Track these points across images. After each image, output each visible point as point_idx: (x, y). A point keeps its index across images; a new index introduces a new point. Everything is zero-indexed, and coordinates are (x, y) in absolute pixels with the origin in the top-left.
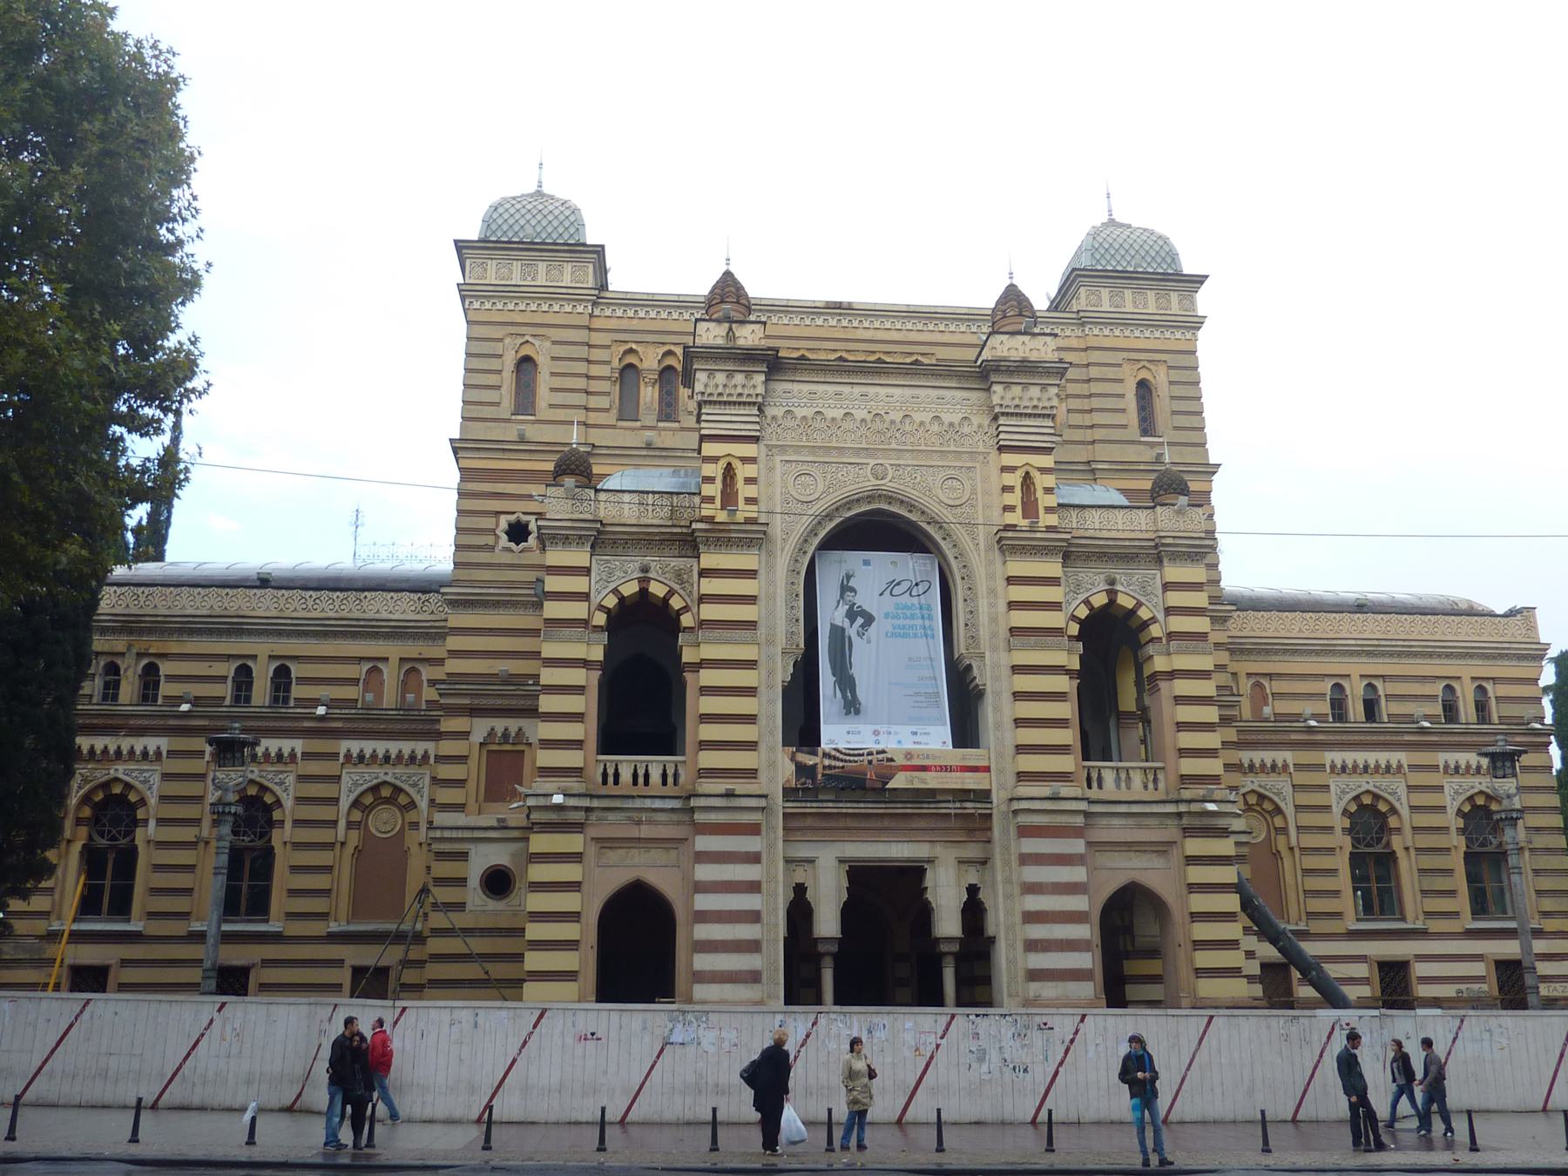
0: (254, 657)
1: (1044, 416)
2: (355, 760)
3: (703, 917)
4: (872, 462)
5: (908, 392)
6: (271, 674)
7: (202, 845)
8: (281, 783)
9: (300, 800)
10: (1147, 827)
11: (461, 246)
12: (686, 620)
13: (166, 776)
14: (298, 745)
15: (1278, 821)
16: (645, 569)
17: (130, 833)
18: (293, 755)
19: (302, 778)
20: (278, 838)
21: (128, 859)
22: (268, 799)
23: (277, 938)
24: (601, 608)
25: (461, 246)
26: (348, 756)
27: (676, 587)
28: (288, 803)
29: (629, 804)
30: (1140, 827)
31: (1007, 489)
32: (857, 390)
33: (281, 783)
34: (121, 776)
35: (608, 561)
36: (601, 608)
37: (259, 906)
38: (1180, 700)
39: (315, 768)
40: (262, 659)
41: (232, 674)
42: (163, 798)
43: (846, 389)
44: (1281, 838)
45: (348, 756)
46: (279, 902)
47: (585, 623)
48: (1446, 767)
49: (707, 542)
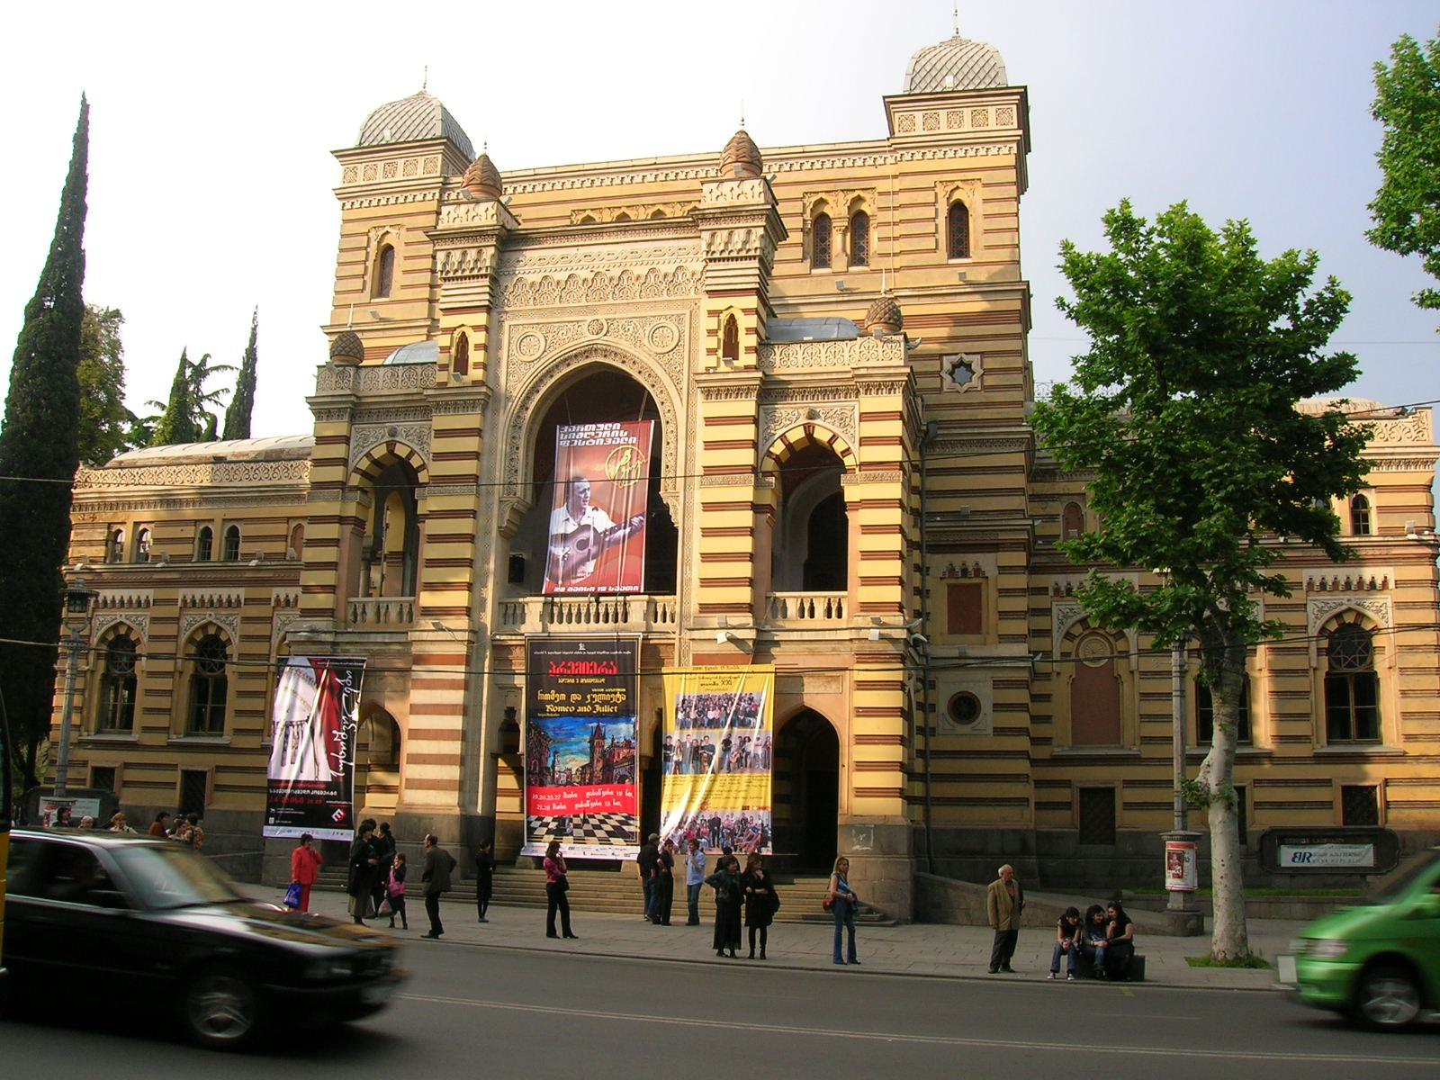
0: (211, 521)
1: (750, 258)
2: (283, 604)
3: (416, 734)
4: (590, 318)
5: (629, 247)
6: (225, 534)
7: (177, 675)
8: (231, 624)
9: (246, 638)
10: (820, 653)
11: (340, 154)
12: (423, 477)
13: (154, 620)
14: (240, 592)
15: (1120, 645)
16: (393, 433)
17: (132, 665)
18: (238, 601)
19: (247, 620)
20: (230, 670)
21: (222, 684)
22: (223, 637)
23: (226, 749)
24: (356, 470)
25: (340, 154)
26: (278, 600)
27: (417, 449)
28: (236, 640)
29: (365, 639)
30: (813, 653)
31: (712, 333)
32: (583, 250)
33: (231, 624)
34: (123, 620)
35: (364, 429)
36: (356, 470)
37: (217, 724)
38: (868, 529)
39: (253, 611)
40: (218, 522)
41: (198, 535)
42: (153, 638)
43: (573, 251)
44: (1122, 662)
45: (278, 600)
46: (230, 721)
47: (342, 485)
48: (1310, 584)
49: (438, 406)
